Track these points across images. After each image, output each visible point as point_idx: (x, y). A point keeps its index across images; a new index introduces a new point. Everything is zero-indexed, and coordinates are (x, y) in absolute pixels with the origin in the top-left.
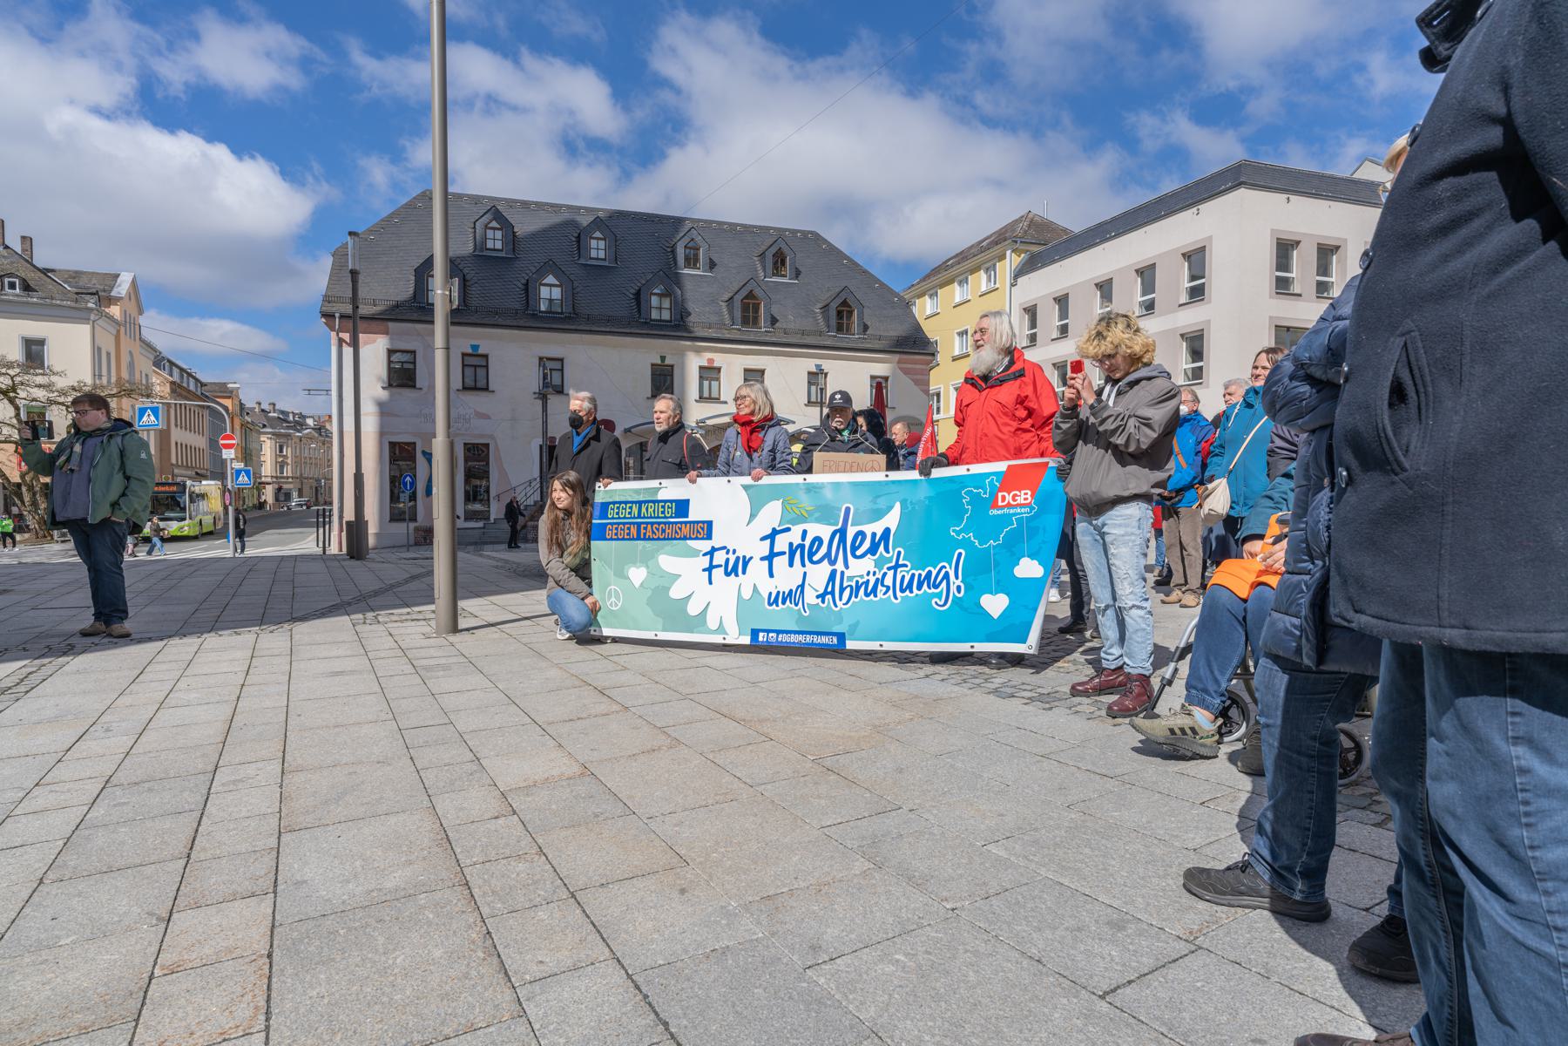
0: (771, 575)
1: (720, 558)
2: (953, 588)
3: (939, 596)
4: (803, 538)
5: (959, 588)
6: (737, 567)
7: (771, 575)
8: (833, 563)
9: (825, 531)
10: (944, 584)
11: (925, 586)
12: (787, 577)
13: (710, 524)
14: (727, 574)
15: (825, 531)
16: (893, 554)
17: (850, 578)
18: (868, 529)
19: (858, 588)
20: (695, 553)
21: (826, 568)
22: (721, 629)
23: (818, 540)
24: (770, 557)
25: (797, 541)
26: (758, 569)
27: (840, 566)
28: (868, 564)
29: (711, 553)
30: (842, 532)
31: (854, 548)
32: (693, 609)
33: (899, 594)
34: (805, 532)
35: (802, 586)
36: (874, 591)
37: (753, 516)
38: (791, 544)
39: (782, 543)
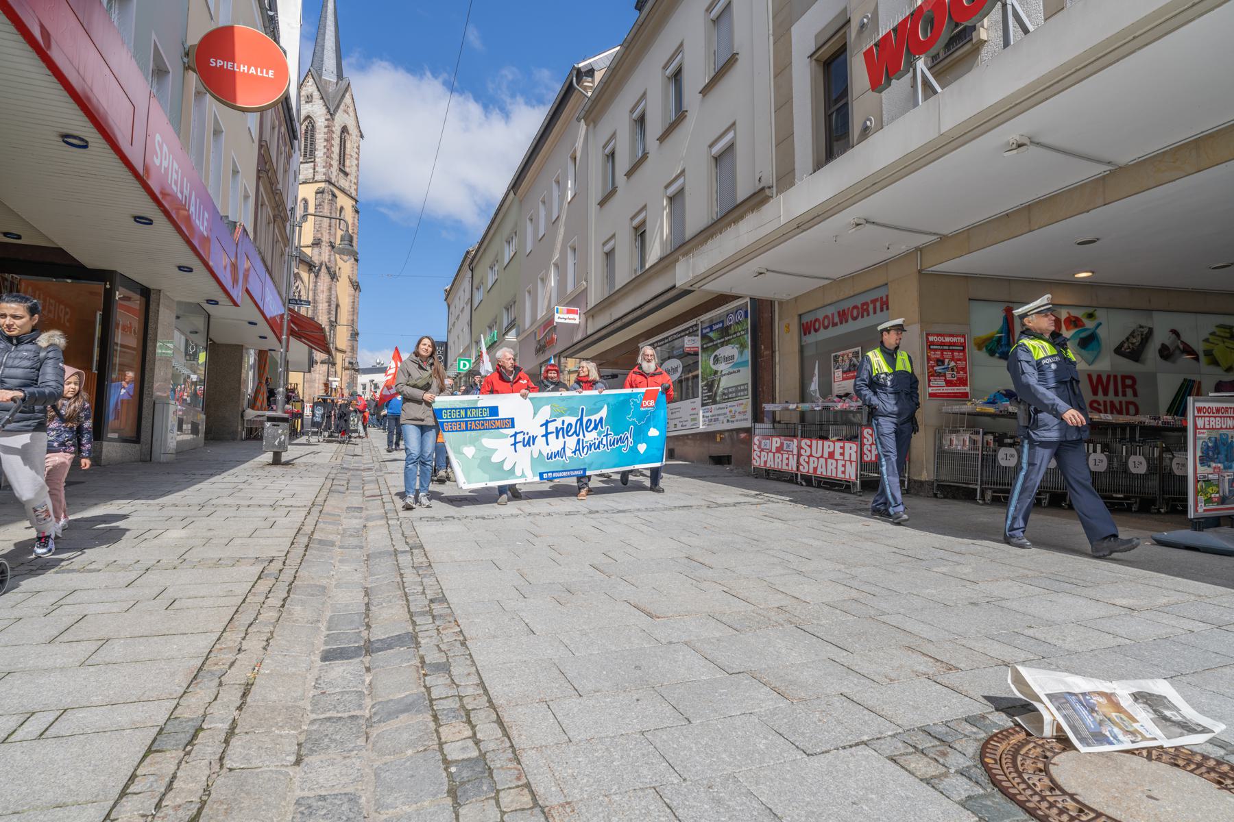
1: (520, 437)
6: (530, 441)
9: (572, 420)
12: (555, 444)
13: (512, 419)
16: (605, 429)
18: (593, 418)
20: (506, 436)
23: (570, 424)
24: (546, 435)
25: (560, 426)
26: (540, 441)
28: (594, 434)
29: (515, 435)
30: (581, 419)
32: (507, 467)
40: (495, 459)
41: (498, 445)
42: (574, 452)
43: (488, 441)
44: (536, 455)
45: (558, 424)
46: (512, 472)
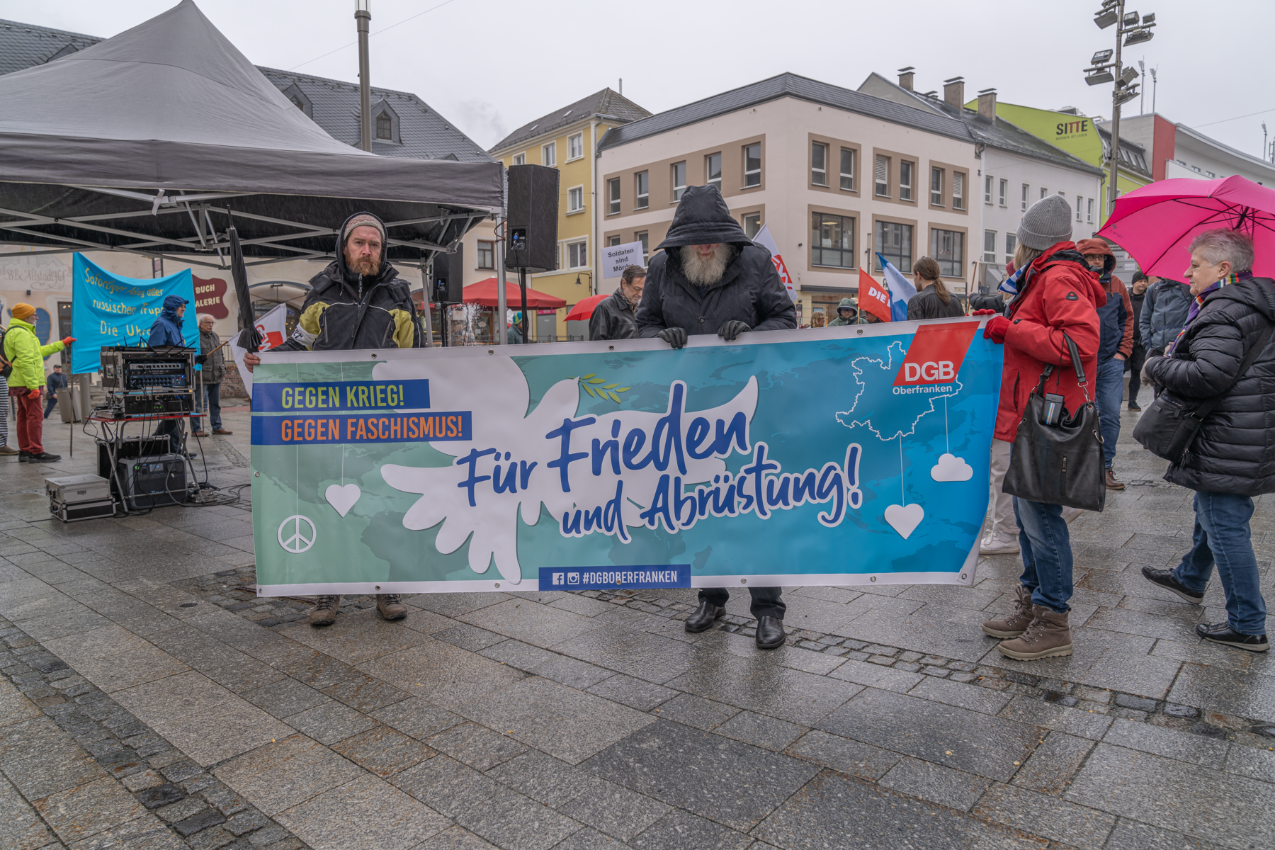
0: (566, 488)
1: (485, 466)
2: (847, 497)
3: (827, 508)
4: (615, 431)
5: (855, 497)
6: (513, 478)
7: (566, 488)
8: (661, 466)
9: (646, 421)
10: (834, 491)
11: (806, 496)
13: (466, 417)
14: (499, 489)
15: (646, 421)
16: (751, 450)
17: (690, 487)
18: (711, 415)
19: (703, 499)
20: (444, 461)
21: (651, 475)
22: (492, 571)
23: (638, 434)
25: (605, 436)
26: (545, 481)
27: (672, 470)
29: (475, 454)
30: (674, 420)
31: (692, 445)
32: (445, 543)
33: (767, 507)
34: (617, 425)
35: (617, 502)
36: (729, 504)
37: (533, 403)
38: (596, 442)
39: (581, 440)
40: (415, 520)
41: (426, 490)
42: (649, 515)
43: (396, 475)
44: (531, 517)
45: (601, 430)
46: (458, 561)
